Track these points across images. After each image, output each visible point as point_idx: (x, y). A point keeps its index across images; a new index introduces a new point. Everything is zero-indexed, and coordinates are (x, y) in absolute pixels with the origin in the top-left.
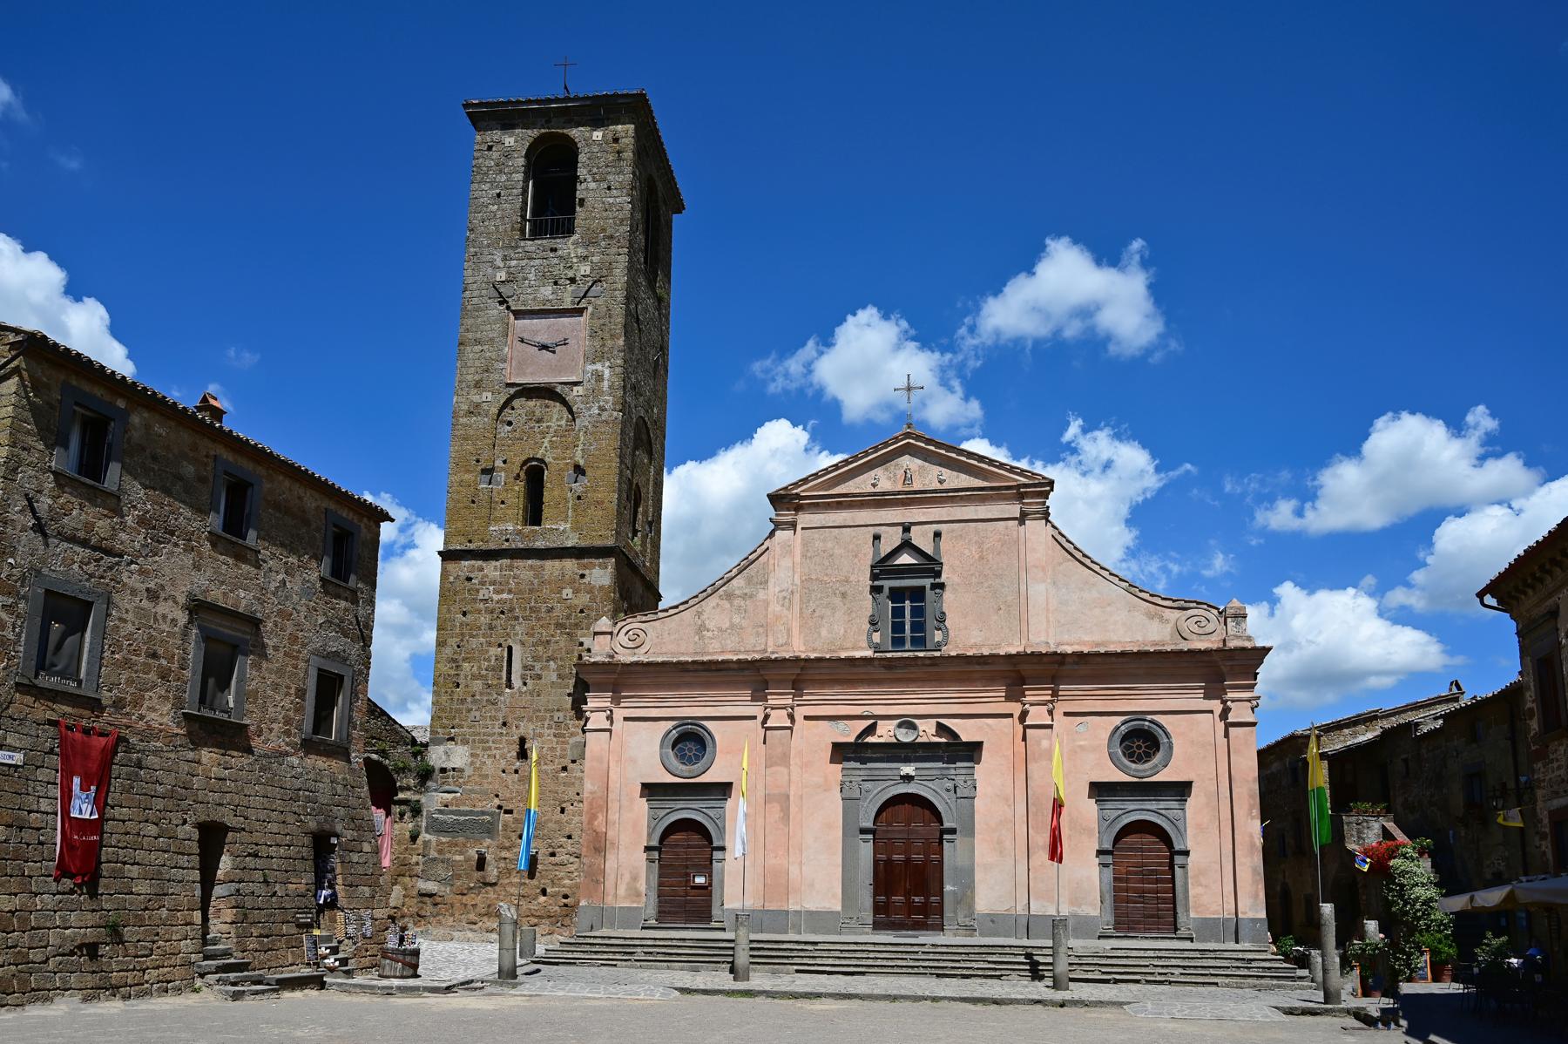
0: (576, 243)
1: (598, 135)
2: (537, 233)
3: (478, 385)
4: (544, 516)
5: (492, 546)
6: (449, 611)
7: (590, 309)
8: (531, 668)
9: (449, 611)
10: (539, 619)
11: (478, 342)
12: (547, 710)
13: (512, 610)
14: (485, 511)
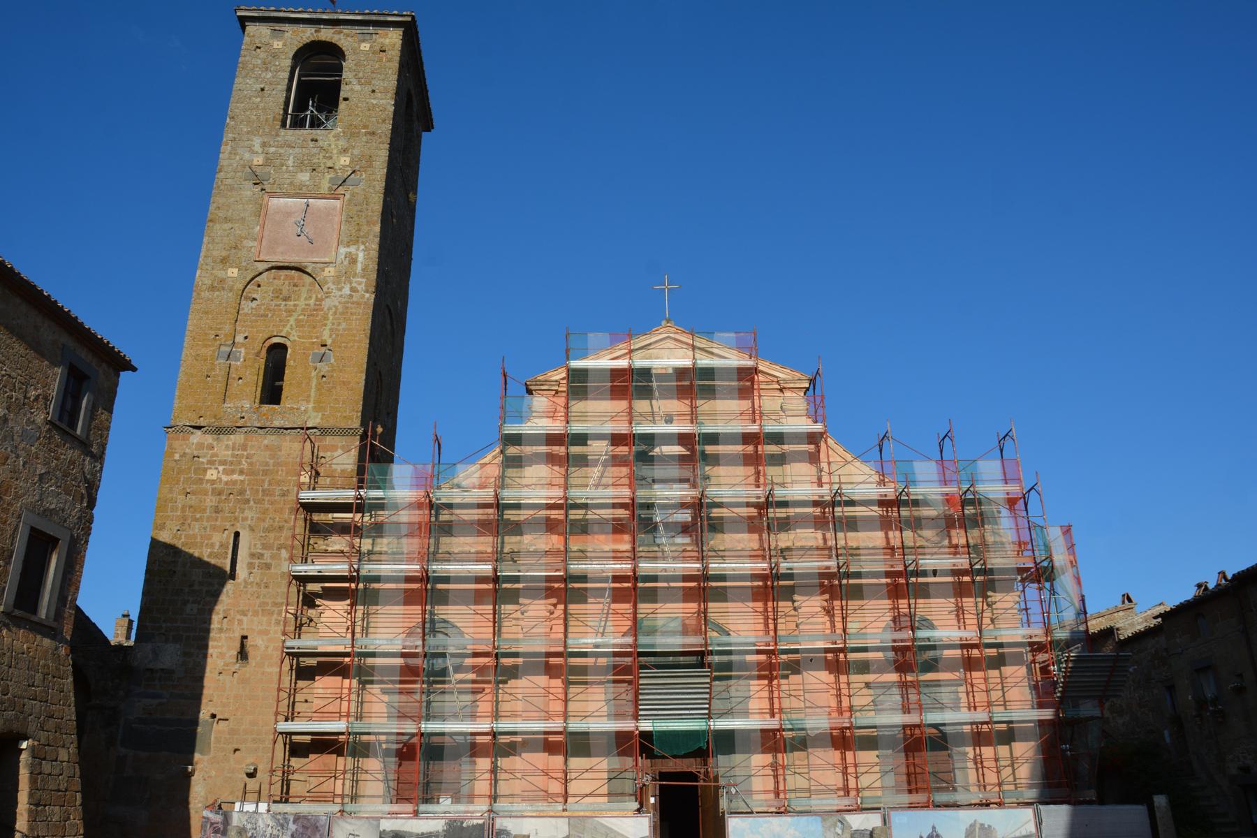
0: (337, 137)
1: (365, 46)
2: (298, 123)
3: (224, 261)
5: (225, 423)
7: (348, 196)
8: (261, 556)
9: (171, 491)
11: (227, 220)
12: (275, 604)
13: (242, 492)
14: (220, 387)
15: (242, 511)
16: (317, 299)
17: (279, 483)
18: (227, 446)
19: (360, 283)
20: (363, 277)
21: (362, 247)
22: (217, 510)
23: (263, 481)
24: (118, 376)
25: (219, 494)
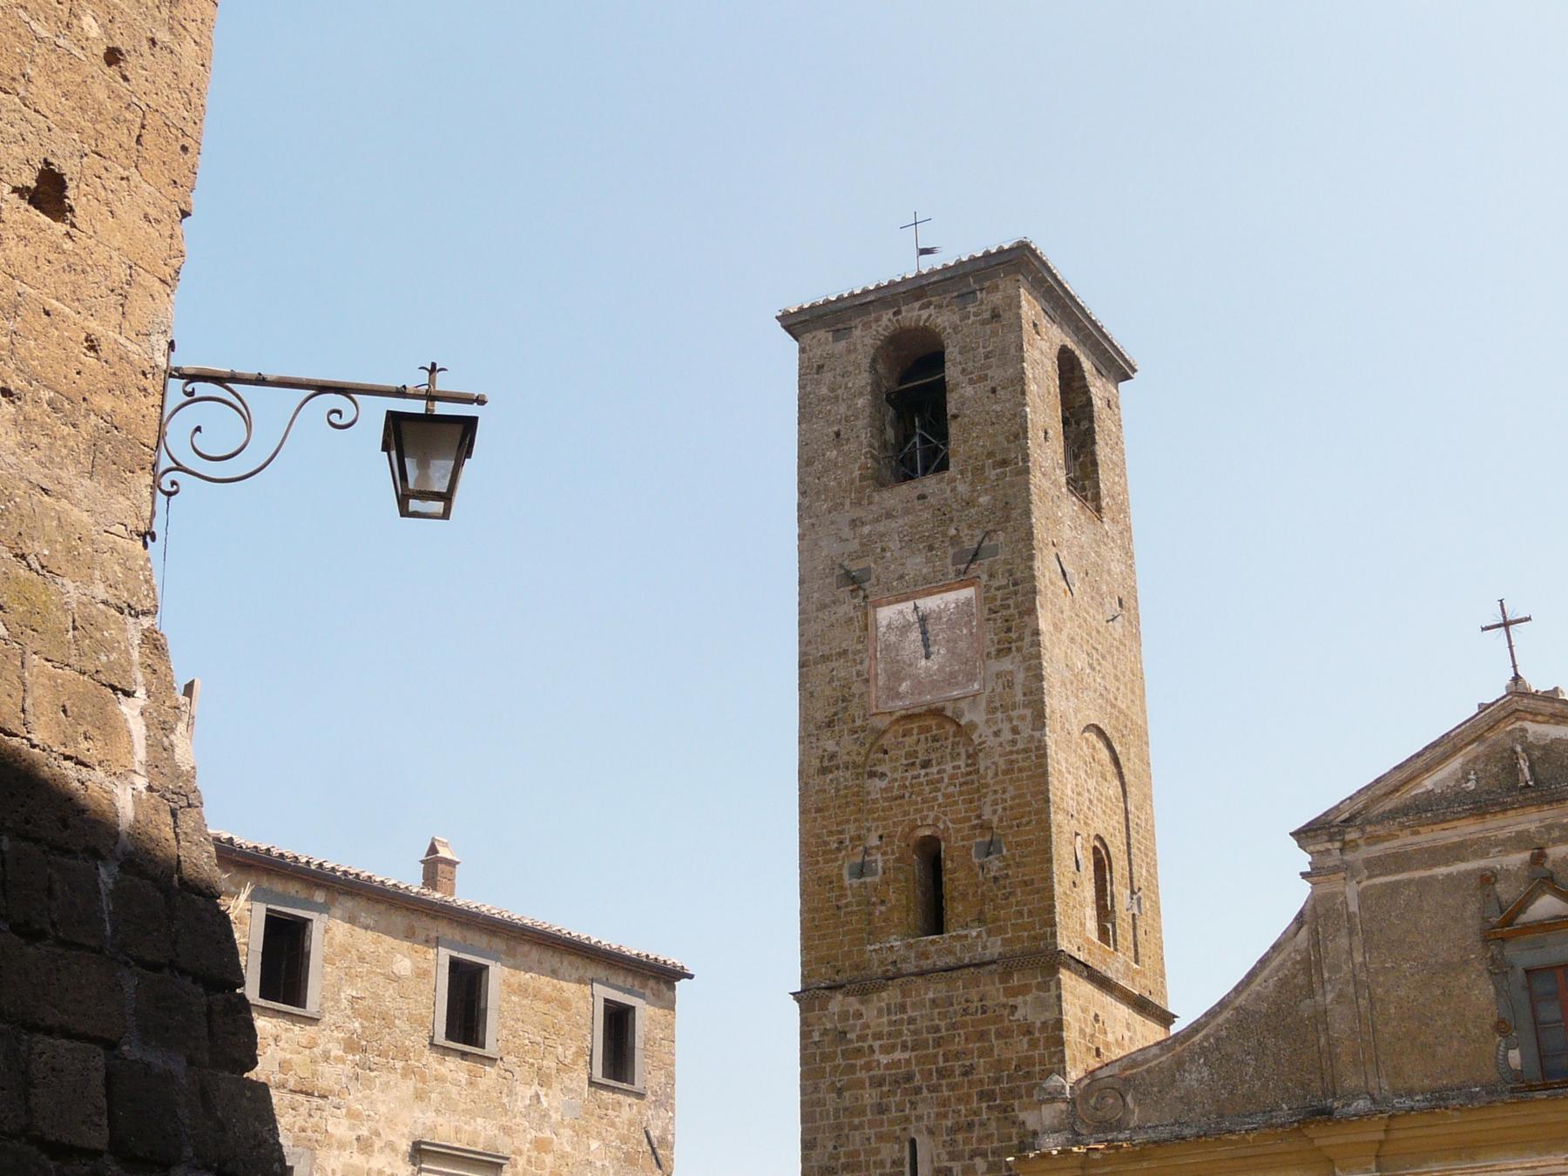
4: (948, 914)
6: (816, 1089)
10: (952, 1087)
11: (825, 658)
13: (909, 1077)
15: (913, 1105)
16: (969, 757)
17: (957, 1056)
18: (880, 1010)
19: (1023, 718)
20: (1025, 706)
21: (1019, 657)
22: (881, 1109)
23: (936, 1056)
24: (674, 988)
25: (880, 1085)
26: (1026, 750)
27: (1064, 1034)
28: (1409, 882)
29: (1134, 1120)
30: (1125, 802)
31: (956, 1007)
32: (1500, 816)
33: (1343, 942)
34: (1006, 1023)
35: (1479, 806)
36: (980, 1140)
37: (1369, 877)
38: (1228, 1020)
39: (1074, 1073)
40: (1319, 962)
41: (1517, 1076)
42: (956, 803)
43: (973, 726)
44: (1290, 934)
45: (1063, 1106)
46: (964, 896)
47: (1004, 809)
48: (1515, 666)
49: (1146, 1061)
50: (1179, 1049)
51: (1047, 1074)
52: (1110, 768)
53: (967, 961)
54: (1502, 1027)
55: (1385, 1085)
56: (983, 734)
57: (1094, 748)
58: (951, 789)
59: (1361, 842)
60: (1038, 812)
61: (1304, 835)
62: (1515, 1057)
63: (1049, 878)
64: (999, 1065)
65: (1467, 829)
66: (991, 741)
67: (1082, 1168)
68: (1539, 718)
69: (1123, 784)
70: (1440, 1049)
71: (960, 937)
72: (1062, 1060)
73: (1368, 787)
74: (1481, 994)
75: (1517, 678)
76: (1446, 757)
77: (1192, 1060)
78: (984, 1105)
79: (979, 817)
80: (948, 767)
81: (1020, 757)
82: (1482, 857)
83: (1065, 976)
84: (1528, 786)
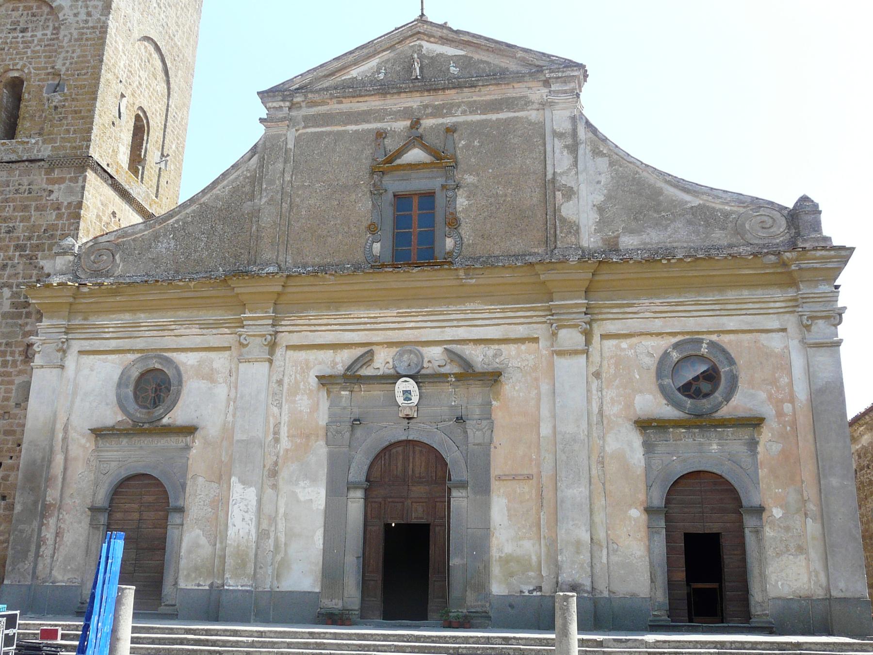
16: (55, 28)
19: (96, 7)
26: (93, 28)
27: (82, 212)
28: (329, 133)
29: (118, 271)
30: (168, 100)
31: (11, 188)
32: (396, 96)
33: (280, 166)
34: (44, 202)
35: (384, 89)
36: (9, 277)
37: (304, 128)
38: (194, 211)
39: (84, 238)
40: (261, 178)
41: (376, 259)
42: (39, 57)
43: (61, 8)
44: (246, 158)
45: (71, 258)
46: (32, 117)
47: (71, 63)
48: (422, 9)
49: (134, 233)
50: (158, 227)
51: (64, 236)
52: (161, 75)
53: (25, 158)
54: (372, 229)
55: (289, 260)
56: (67, 14)
57: (151, 55)
58: (38, 48)
59: (303, 104)
60: (94, 67)
61: (265, 95)
62: (377, 247)
63: (92, 111)
64: (33, 228)
65: (374, 103)
66: (71, 19)
67: (75, 298)
68: (432, 39)
69: (169, 89)
70: (329, 239)
71: (23, 143)
72: (77, 229)
73: (315, 69)
74: (362, 206)
75: (423, 15)
76: (369, 57)
77: (165, 235)
78: (17, 254)
79: (53, 68)
80: (39, 34)
81: (88, 31)
82: (380, 121)
83: (90, 175)
84: (417, 78)
